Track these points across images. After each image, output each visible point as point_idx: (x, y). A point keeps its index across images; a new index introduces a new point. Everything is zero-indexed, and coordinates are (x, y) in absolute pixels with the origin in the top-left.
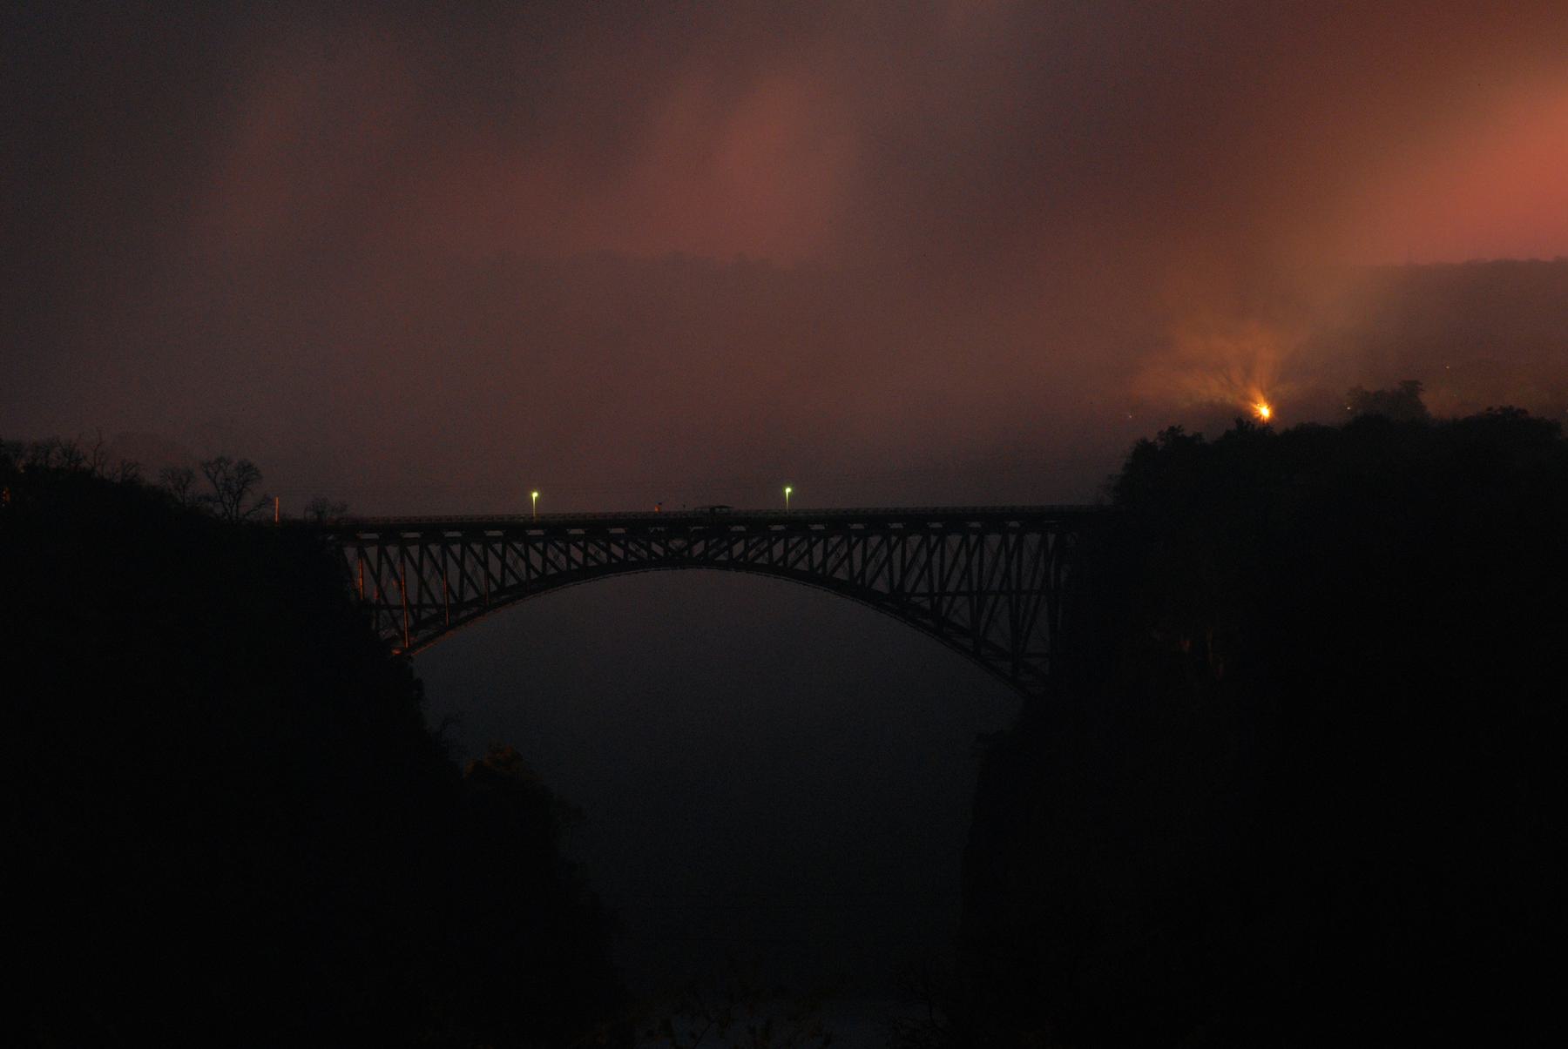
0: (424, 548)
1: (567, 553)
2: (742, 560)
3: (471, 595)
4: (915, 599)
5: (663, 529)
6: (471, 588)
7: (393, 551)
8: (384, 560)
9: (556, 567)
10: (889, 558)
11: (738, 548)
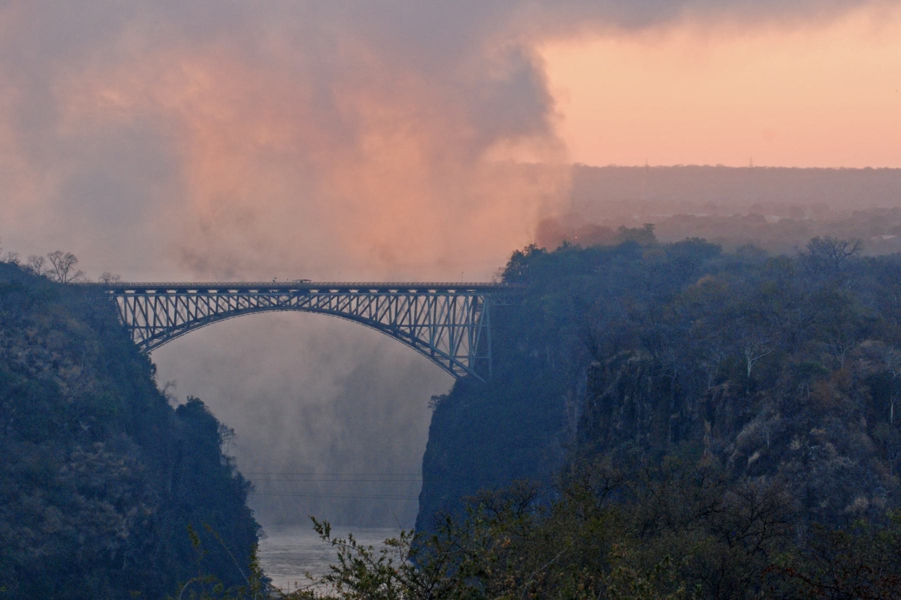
0: (157, 298)
1: (228, 302)
2: (316, 307)
3: (180, 322)
4: (402, 328)
5: (277, 291)
6: (180, 319)
7: (141, 299)
8: (137, 304)
9: (223, 309)
10: (389, 308)
11: (314, 301)
